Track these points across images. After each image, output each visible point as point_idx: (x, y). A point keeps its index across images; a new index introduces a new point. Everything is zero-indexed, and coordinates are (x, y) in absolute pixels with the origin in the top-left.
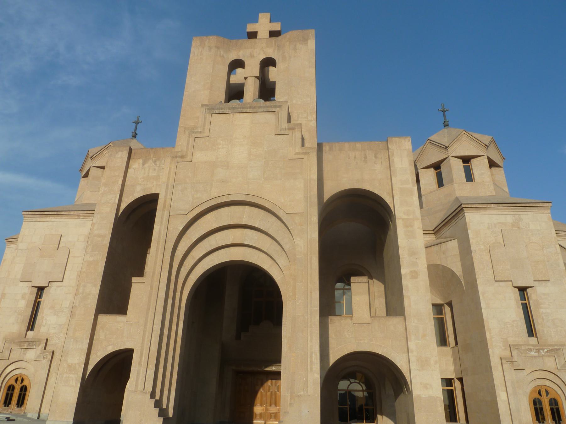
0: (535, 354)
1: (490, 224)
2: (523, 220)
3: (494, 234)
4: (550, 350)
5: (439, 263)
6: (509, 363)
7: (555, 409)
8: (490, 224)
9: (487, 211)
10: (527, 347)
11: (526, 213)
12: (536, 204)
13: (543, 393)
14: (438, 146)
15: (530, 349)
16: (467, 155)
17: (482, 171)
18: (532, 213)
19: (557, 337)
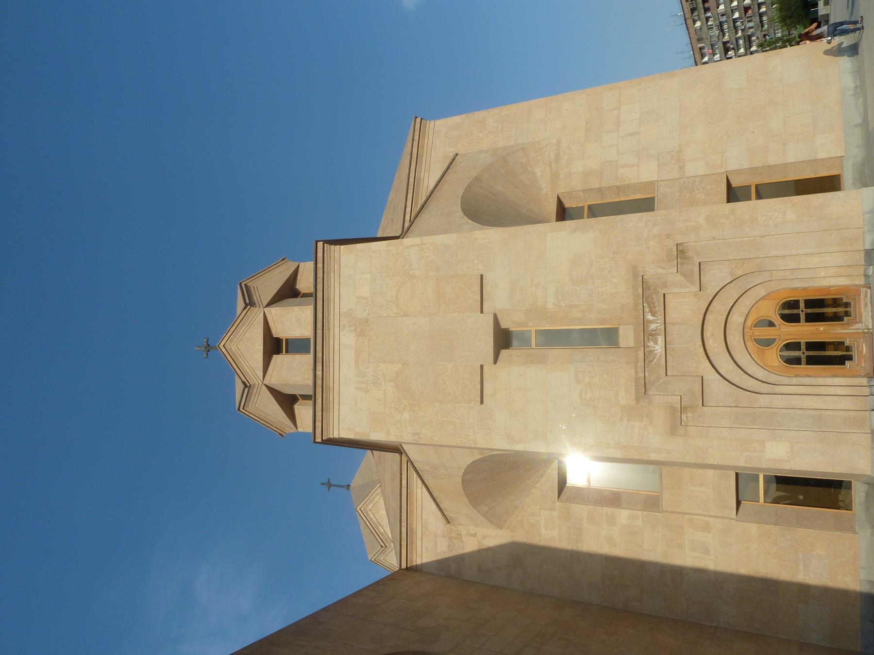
0: (659, 343)
1: (359, 385)
2: (352, 310)
3: (380, 381)
4: (649, 306)
5: (460, 480)
6: (684, 418)
7: (809, 311)
8: (359, 385)
9: (331, 385)
10: (641, 364)
11: (337, 300)
12: (318, 276)
13: (766, 333)
14: (247, 402)
15: (648, 355)
16: (262, 347)
17: (294, 320)
18: (337, 285)
19: (614, 280)
